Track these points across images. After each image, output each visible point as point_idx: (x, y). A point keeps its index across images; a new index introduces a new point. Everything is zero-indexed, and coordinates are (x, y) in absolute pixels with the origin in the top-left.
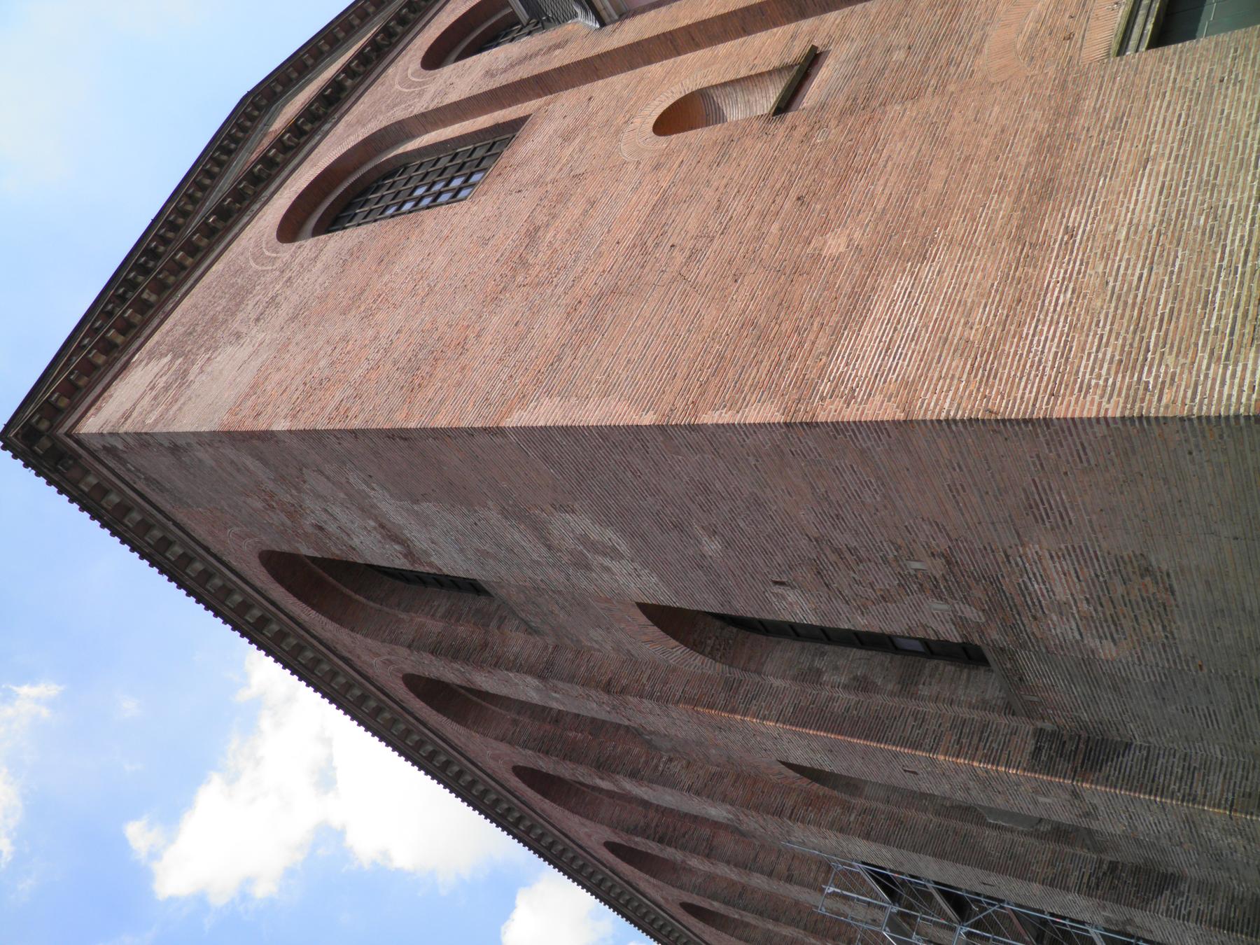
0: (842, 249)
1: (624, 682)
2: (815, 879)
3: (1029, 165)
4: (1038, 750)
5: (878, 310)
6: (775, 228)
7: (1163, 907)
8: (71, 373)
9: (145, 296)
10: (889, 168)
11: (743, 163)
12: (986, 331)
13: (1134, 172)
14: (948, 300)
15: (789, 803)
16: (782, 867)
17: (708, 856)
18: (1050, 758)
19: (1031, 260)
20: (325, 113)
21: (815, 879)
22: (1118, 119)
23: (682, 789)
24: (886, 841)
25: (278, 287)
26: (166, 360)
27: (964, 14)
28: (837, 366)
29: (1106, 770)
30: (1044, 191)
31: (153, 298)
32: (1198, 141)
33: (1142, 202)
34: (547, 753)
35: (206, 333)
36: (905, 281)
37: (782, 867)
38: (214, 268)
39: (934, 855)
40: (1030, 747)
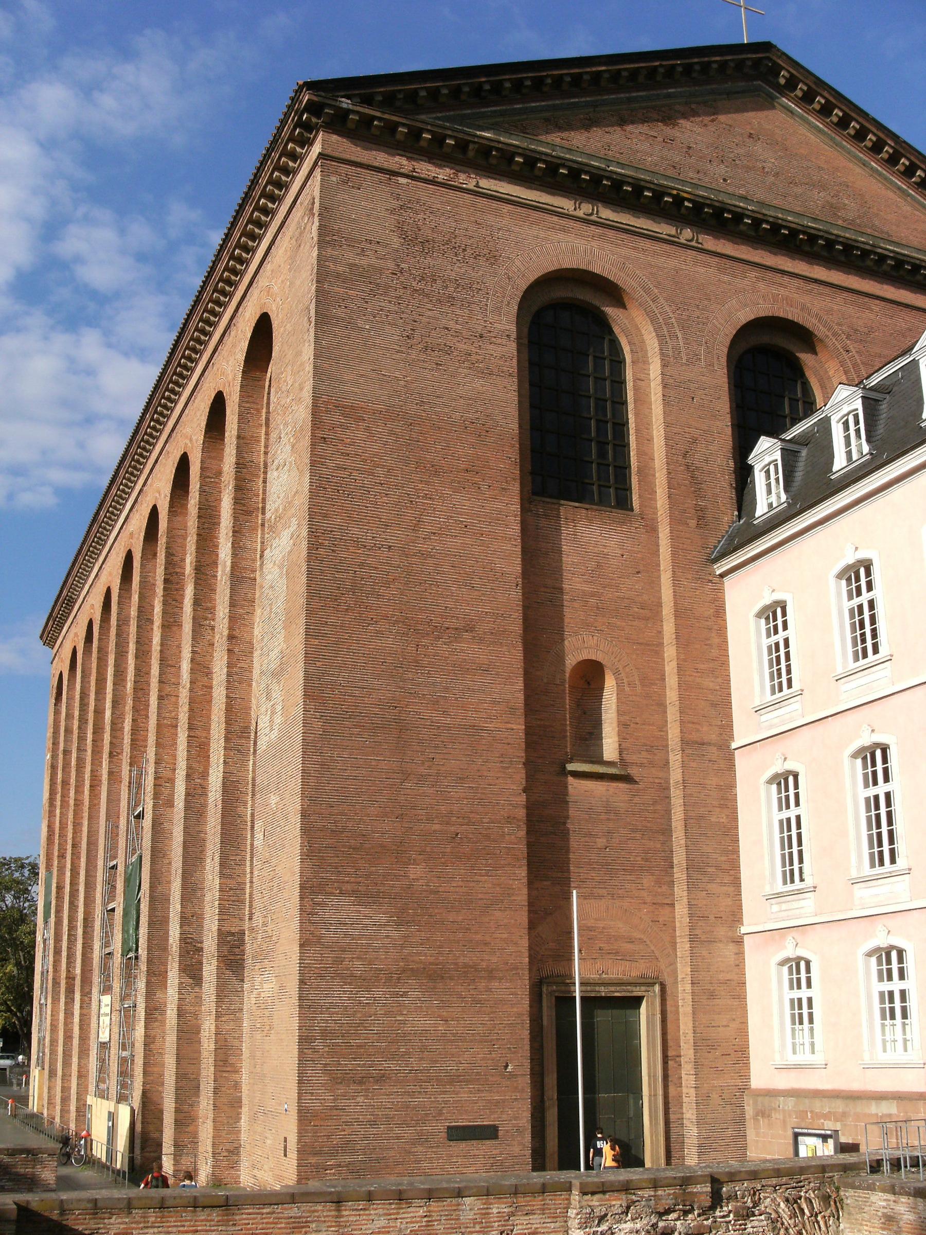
0: (412, 876)
1: (236, 650)
2: (164, 718)
3: (456, 964)
4: (233, 934)
5: (366, 911)
6: (437, 827)
7: (183, 981)
8: (380, 119)
9: (471, 146)
10: (472, 884)
11: (500, 780)
12: (348, 969)
13: (439, 1016)
14: (369, 945)
15: (198, 733)
16: (168, 689)
17: (163, 626)
18: (229, 942)
19: (389, 979)
20: (704, 220)
21: (164, 718)
22: (479, 1002)
23: (193, 646)
24: (187, 808)
25: (462, 346)
26: (396, 241)
27: (629, 877)
28: (333, 901)
29: (227, 972)
30: (434, 976)
31: (471, 154)
32: (452, 1041)
33: (420, 1022)
34: (199, 517)
35: (423, 278)
36: (383, 918)
37: (168, 689)
38: (507, 208)
39: (184, 842)
40: (233, 930)
